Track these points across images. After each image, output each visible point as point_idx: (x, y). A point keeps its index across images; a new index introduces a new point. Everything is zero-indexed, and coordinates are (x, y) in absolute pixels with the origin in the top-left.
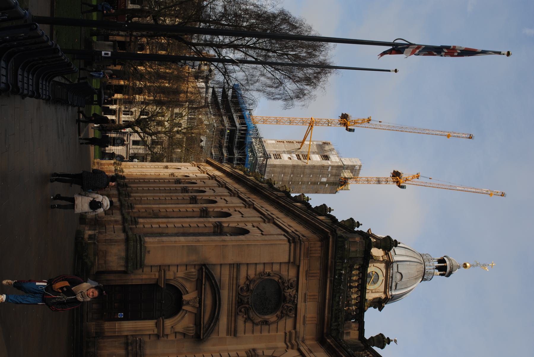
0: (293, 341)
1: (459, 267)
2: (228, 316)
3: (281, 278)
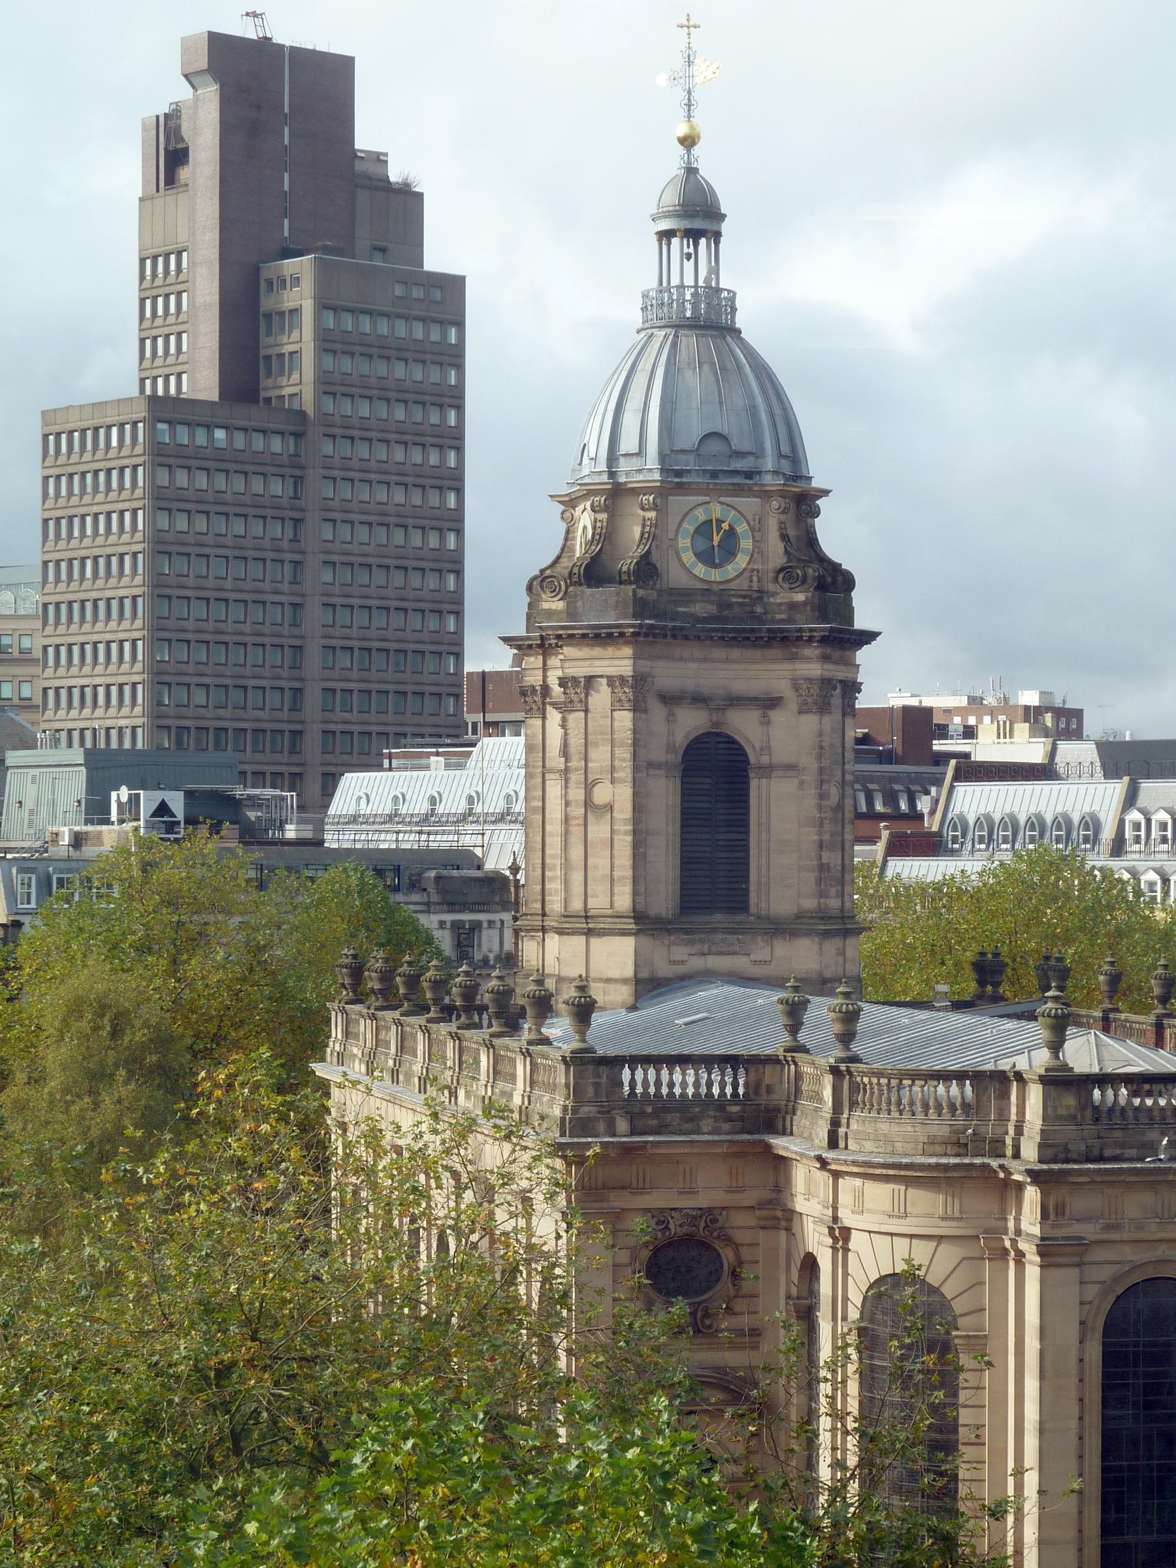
1: (691, 171)
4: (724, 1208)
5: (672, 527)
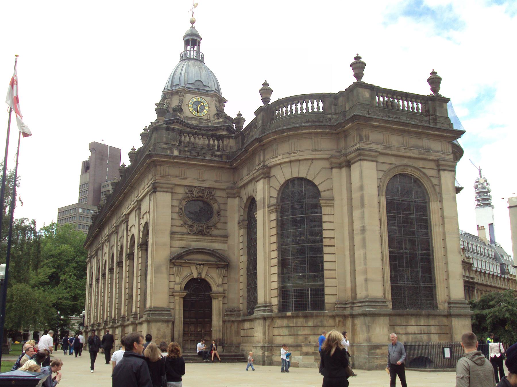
0: (235, 191)
1: (193, 27)
2: (212, 242)
3: (184, 199)
4: (214, 188)
5: (187, 102)
